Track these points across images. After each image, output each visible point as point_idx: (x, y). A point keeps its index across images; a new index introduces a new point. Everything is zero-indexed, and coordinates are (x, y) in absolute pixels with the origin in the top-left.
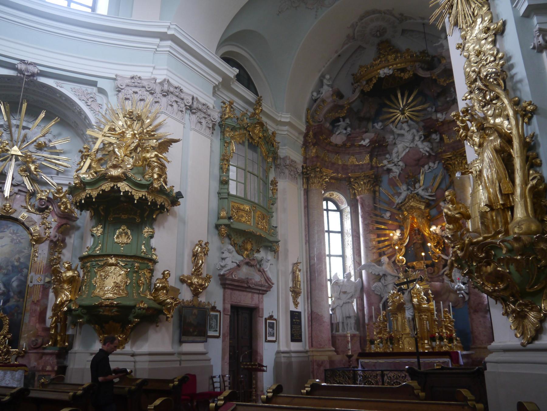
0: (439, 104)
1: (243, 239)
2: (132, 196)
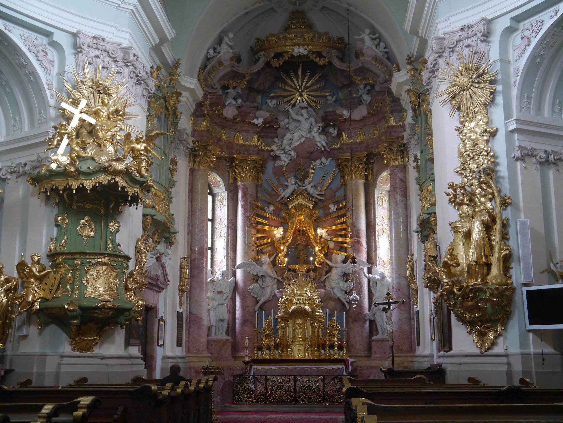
1: (154, 229)
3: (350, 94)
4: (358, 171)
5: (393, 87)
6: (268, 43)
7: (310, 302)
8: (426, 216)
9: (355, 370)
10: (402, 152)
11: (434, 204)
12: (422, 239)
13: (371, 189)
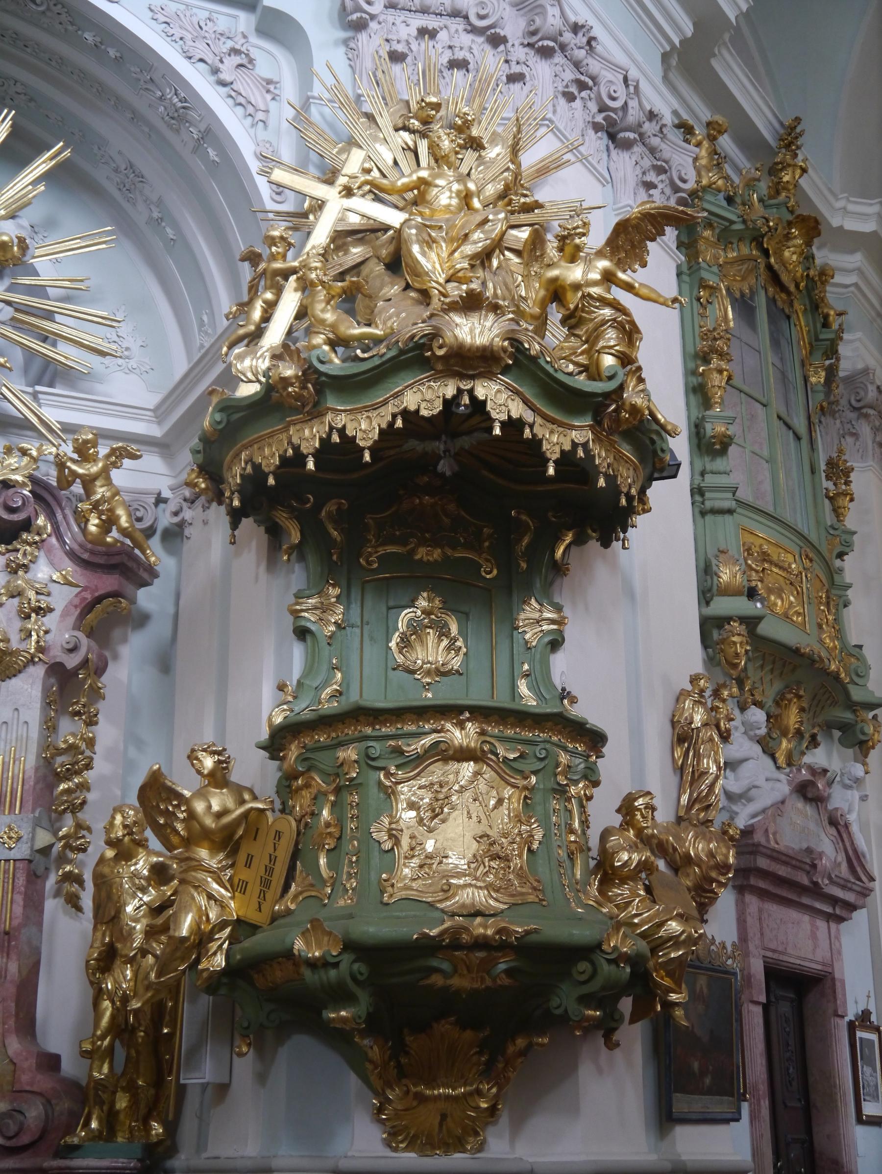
1: (778, 686)
2: (536, 443)
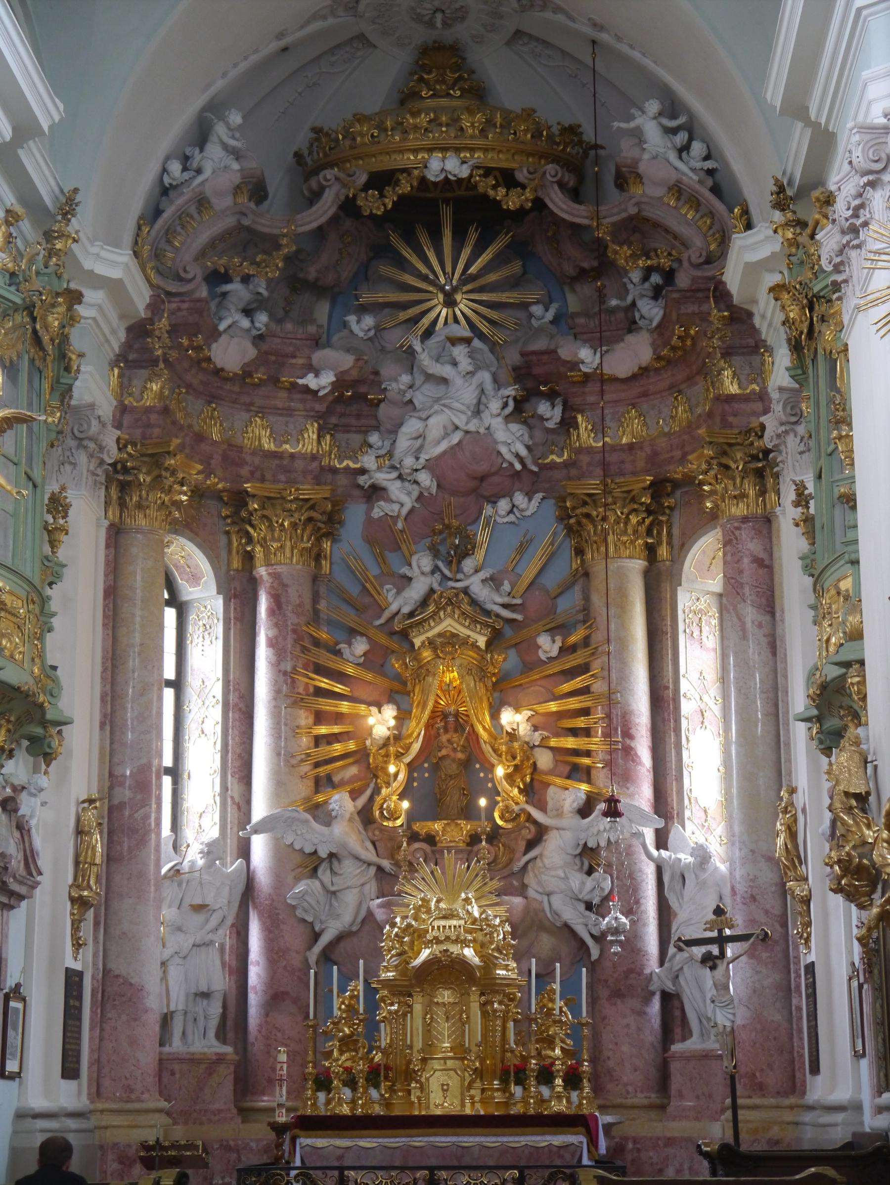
0: (571, 298)
3: (602, 297)
4: (625, 532)
5: (733, 277)
6: (348, 143)
7: (480, 936)
8: (834, 672)
9: (617, 1150)
10: (760, 474)
11: (856, 635)
12: (821, 742)
13: (666, 587)
